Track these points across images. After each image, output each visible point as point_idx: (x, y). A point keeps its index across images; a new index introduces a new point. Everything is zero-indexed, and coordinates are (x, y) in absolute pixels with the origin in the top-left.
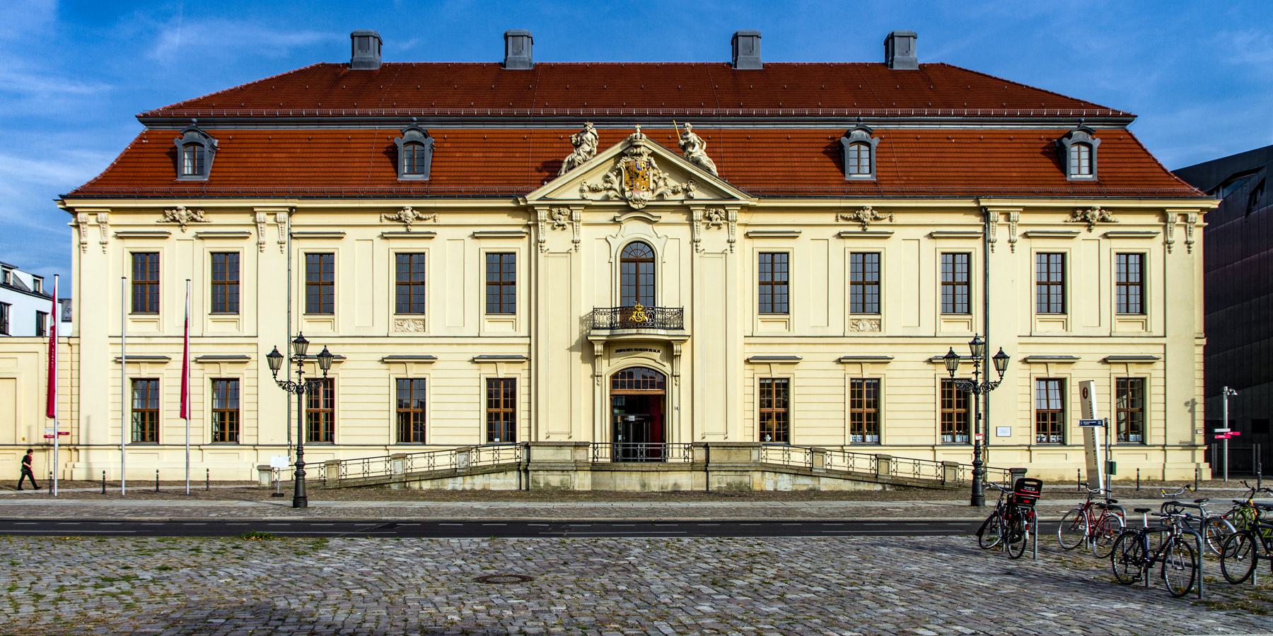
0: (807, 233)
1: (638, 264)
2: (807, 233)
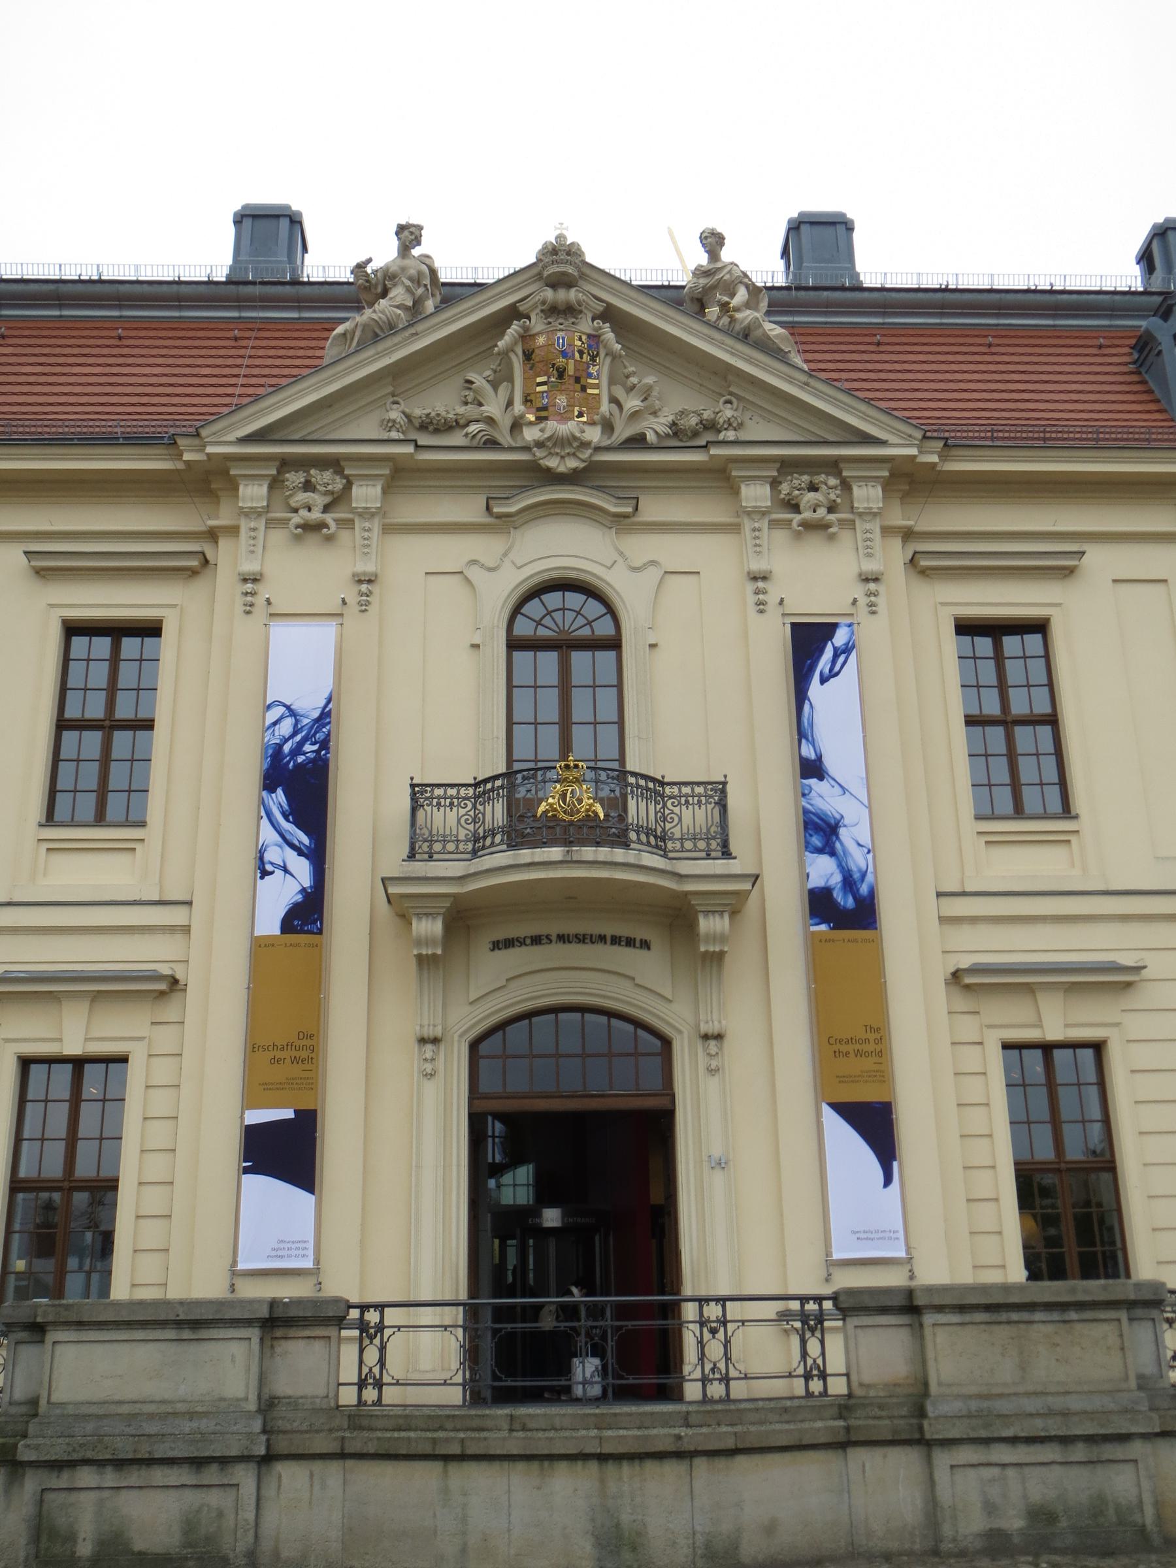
0: (1097, 558)
1: (564, 638)
2: (1100, 561)
